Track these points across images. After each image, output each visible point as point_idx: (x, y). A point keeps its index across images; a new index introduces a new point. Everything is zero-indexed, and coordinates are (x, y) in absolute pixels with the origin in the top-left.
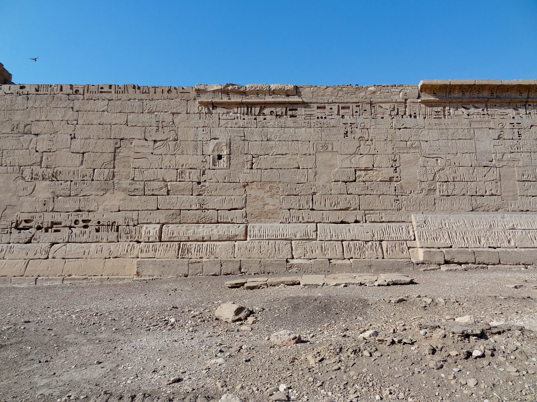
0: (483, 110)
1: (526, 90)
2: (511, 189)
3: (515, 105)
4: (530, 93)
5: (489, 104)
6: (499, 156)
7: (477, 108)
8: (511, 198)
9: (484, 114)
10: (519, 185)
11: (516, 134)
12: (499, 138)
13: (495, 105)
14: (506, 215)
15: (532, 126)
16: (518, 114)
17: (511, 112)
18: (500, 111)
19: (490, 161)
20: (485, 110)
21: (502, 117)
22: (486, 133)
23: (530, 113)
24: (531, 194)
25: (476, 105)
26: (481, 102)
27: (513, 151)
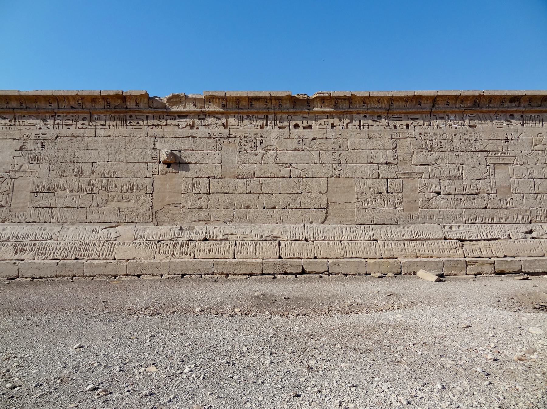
0: (10, 121)
1: (55, 101)
2: (22, 201)
3: (44, 115)
4: (60, 104)
5: (17, 115)
6: (17, 167)
7: (5, 118)
8: (19, 210)
9: (11, 125)
10: (31, 197)
11: (40, 145)
12: (21, 149)
13: (24, 116)
14: (9, 227)
15: (57, 137)
16: (46, 125)
17: (39, 123)
18: (27, 122)
19: (7, 172)
20: (13, 120)
21: (28, 128)
22: (8, 144)
23: (58, 124)
24: (41, 206)
25: (4, 116)
26: (9, 113)
27: (33, 162)
